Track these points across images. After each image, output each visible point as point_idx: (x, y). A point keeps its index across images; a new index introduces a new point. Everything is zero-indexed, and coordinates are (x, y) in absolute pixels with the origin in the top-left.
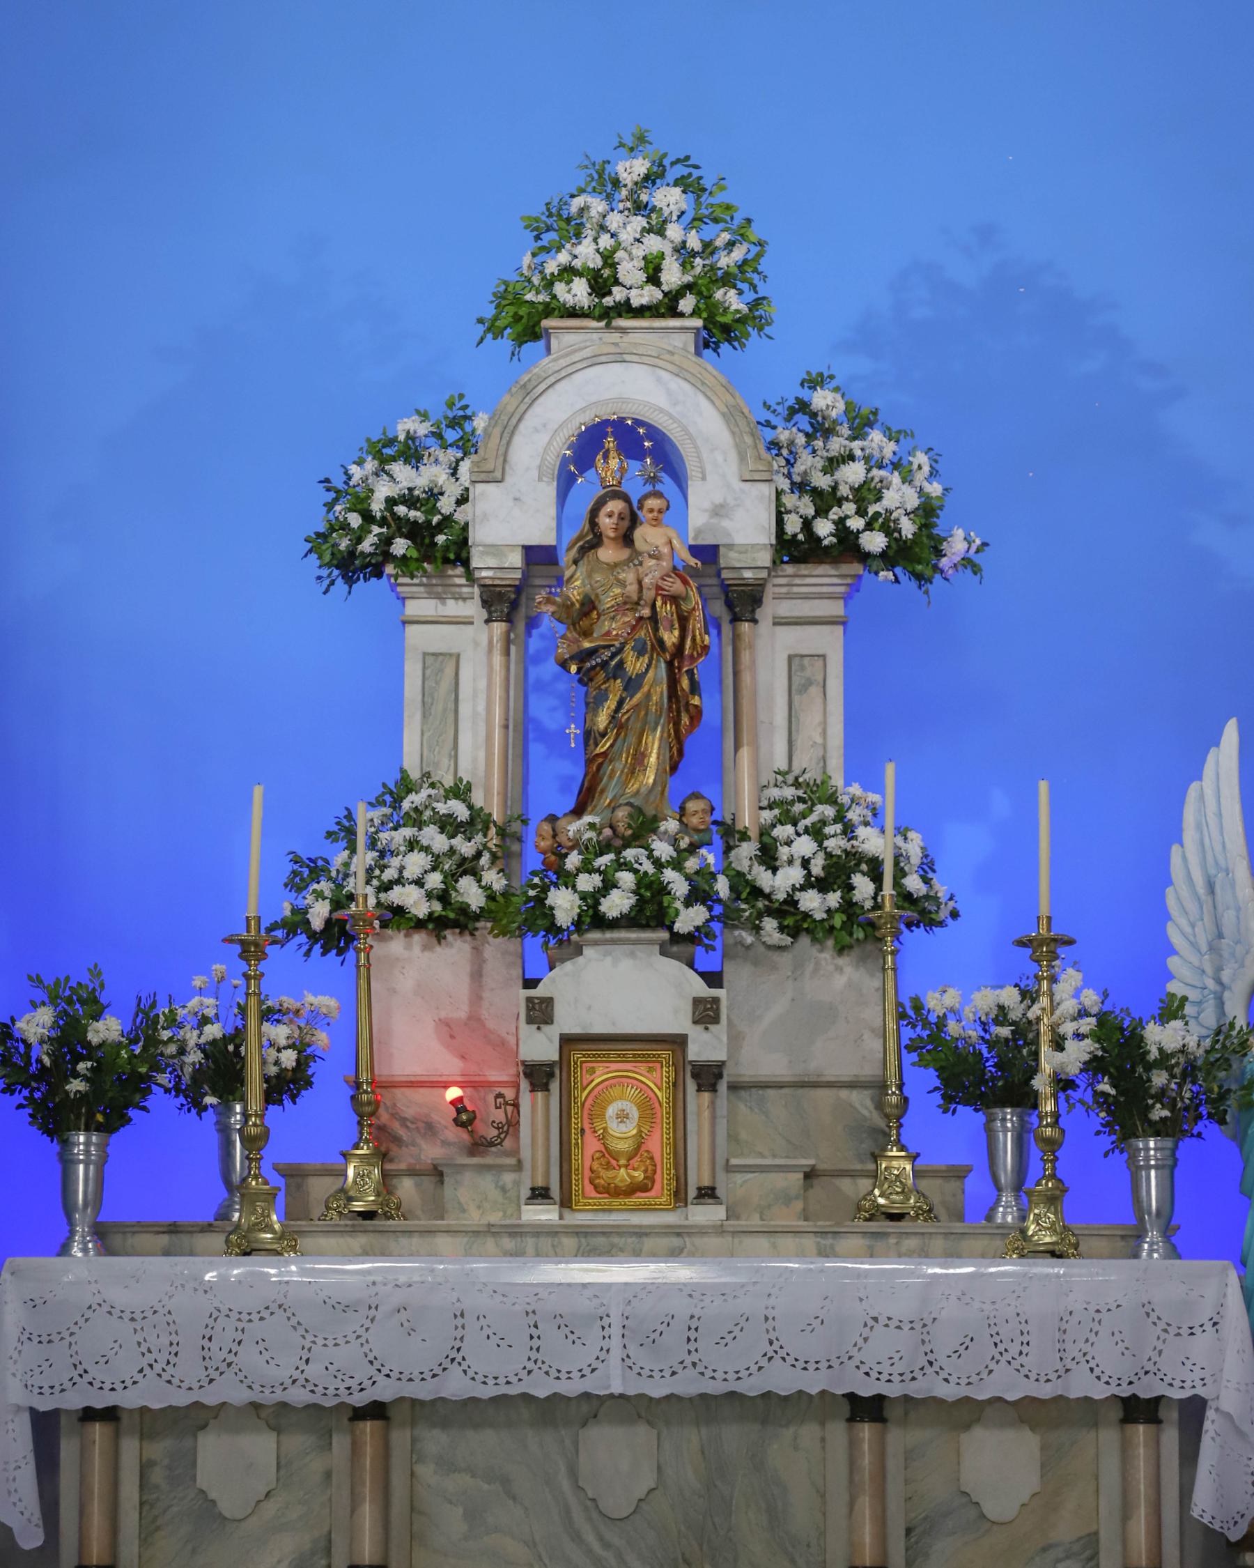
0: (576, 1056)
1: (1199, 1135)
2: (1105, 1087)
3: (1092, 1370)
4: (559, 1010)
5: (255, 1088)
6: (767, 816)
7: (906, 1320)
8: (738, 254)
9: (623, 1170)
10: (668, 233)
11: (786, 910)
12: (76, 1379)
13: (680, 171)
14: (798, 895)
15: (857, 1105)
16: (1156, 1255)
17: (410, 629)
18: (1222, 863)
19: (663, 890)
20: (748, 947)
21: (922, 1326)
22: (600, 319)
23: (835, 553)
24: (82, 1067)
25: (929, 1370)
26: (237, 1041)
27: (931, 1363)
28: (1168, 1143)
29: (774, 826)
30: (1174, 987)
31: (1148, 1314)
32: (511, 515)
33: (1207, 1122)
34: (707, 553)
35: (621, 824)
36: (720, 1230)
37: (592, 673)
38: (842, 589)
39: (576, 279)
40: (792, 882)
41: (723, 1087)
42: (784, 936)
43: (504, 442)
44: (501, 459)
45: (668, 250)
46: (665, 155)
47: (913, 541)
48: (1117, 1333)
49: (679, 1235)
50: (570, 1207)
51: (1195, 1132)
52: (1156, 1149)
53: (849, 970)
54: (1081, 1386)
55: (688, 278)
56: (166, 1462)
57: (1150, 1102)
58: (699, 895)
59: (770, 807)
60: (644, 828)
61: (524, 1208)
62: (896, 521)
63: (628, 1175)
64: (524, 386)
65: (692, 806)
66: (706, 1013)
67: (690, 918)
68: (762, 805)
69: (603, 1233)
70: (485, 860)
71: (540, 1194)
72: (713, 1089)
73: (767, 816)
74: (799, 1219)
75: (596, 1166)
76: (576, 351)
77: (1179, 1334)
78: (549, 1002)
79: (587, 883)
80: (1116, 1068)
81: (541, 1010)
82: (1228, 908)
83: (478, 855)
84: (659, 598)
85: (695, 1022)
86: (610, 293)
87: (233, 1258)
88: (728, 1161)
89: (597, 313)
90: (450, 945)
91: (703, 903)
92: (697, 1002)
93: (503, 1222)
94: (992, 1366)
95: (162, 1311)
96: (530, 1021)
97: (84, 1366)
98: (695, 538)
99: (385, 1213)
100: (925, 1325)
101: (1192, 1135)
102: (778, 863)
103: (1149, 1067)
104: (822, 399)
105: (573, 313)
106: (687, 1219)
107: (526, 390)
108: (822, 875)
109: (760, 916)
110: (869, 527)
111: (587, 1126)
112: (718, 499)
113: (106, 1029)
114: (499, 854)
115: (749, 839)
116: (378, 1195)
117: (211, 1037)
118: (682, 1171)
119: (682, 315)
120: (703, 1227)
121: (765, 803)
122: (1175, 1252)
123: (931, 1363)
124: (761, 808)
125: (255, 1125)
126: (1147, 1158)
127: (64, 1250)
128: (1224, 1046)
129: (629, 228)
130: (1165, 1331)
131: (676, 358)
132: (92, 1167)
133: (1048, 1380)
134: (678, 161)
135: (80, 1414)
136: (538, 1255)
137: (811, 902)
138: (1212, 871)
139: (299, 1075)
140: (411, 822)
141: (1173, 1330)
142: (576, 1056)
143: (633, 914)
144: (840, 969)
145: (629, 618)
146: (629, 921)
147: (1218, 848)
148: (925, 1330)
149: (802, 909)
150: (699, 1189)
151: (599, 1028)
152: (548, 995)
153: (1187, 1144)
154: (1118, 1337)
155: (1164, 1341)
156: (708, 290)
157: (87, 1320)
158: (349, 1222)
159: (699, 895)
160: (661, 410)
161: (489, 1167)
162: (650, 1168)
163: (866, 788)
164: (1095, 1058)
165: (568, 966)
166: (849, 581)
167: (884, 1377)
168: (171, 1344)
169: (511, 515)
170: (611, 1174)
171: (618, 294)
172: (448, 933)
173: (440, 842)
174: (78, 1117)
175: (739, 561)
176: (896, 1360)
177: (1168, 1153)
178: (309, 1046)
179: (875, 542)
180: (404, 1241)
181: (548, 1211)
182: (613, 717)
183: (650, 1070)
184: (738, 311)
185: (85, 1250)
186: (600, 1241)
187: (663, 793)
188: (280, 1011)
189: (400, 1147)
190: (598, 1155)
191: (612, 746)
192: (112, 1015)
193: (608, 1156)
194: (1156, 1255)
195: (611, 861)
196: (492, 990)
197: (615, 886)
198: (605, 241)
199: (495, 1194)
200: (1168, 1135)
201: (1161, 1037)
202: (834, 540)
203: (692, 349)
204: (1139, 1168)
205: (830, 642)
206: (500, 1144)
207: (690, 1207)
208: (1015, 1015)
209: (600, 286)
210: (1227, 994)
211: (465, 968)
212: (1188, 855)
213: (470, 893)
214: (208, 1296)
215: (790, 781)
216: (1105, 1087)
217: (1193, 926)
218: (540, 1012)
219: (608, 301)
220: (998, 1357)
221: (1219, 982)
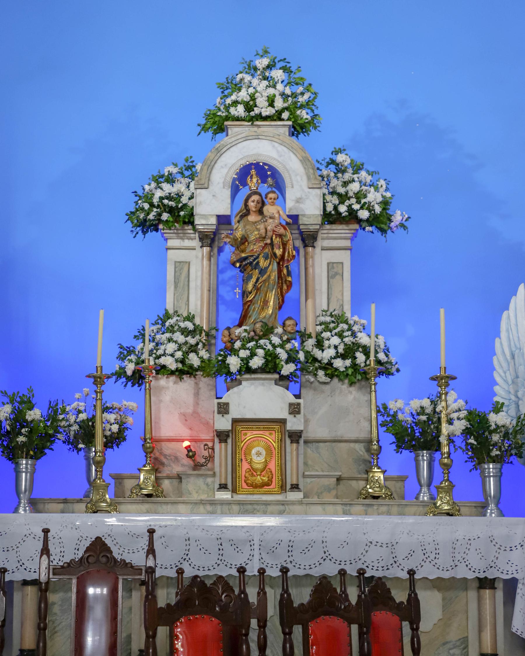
0: (239, 428)
1: (511, 463)
2: (472, 441)
3: (467, 566)
4: (232, 408)
5: (99, 440)
6: (319, 328)
7: (385, 543)
8: (306, 97)
9: (259, 477)
10: (277, 87)
12: (19, 567)
13: (282, 64)
14: (333, 361)
15: (358, 450)
16: (493, 515)
17: (169, 252)
18: (518, 346)
19: (276, 357)
20: (312, 383)
21: (392, 546)
22: (249, 121)
23: (347, 219)
24: (23, 430)
25: (395, 565)
26: (93, 421)
27: (395, 562)
28: (499, 466)
29: (322, 333)
30: (496, 399)
31: (492, 541)
32: (211, 203)
33: (515, 457)
34: (295, 218)
36: (300, 503)
37: (246, 267)
38: (350, 235)
39: (239, 105)
40: (330, 355)
41: (301, 441)
43: (209, 172)
44: (208, 179)
45: (277, 94)
46: (276, 58)
47: (380, 214)
48: (478, 549)
49: (283, 505)
50: (236, 493)
51: (510, 462)
52: (493, 468)
53: (354, 392)
54: (462, 573)
55: (286, 105)
56: (60, 603)
57: (491, 448)
58: (291, 359)
59: (321, 324)
60: (268, 332)
61: (216, 493)
62: (373, 206)
63: (261, 479)
64: (217, 149)
65: (288, 323)
66: (295, 409)
67: (288, 369)
69: (250, 504)
70: (200, 346)
71: (223, 487)
72: (298, 442)
73: (319, 328)
74: (334, 498)
75: (247, 475)
76: (239, 134)
77: (505, 550)
78: (227, 404)
79: (244, 354)
80: (476, 433)
81: (224, 408)
82: (521, 365)
83: (197, 344)
84: (274, 235)
85: (290, 414)
86: (253, 110)
87: (89, 514)
88: (304, 473)
89: (248, 119)
91: (293, 362)
92: (291, 405)
93: (207, 499)
94: (423, 563)
95: (57, 537)
96: (219, 413)
97: (23, 561)
98: (289, 212)
99: (157, 495)
100: (393, 545)
101: (508, 463)
102: (324, 348)
103: (491, 432)
104: (340, 158)
105: (238, 119)
106: (286, 498)
107: (218, 150)
108: (343, 352)
109: (316, 370)
110: (362, 208)
111: (243, 458)
112: (298, 195)
113: (34, 414)
114: (206, 344)
115: (312, 338)
116: (153, 487)
117: (82, 419)
118: (284, 477)
119: (283, 120)
120: (293, 501)
121: (318, 323)
122: (502, 513)
123: (395, 562)
124: (317, 325)
125: (99, 456)
126: (489, 473)
127: (16, 510)
128: (522, 423)
129: (261, 85)
130: (499, 548)
131: (281, 137)
132: (28, 474)
133: (448, 570)
134: (281, 60)
135: (22, 582)
136: (222, 513)
137: (339, 363)
138: (514, 349)
139: (120, 436)
140: (169, 331)
141: (503, 548)
142: (239, 428)
143: (263, 367)
144: (351, 393)
145: (262, 244)
146: (262, 370)
147: (516, 339)
148: (393, 547)
149: (335, 367)
150: (292, 485)
151: (249, 415)
152: (227, 402)
153: (506, 466)
154: (478, 551)
155: (499, 553)
156: (294, 110)
157: (24, 541)
158: (141, 499)
159: (291, 359)
160: (275, 159)
161: (201, 475)
163: (360, 318)
164: (467, 428)
165: (235, 389)
166: (353, 232)
167: (375, 568)
168: (61, 552)
169: (211, 203)
170: (254, 478)
171: (257, 111)
172: (184, 376)
174: (22, 452)
175: (308, 221)
176: (380, 561)
177: (498, 470)
178: (125, 423)
179: (364, 214)
180: (164, 507)
181: (227, 494)
182: (255, 285)
183: (270, 434)
184: (307, 119)
185: (25, 510)
186: (249, 507)
187: (275, 318)
188: (112, 408)
189: (164, 467)
190: (248, 470)
191: (254, 297)
192: (37, 408)
193: (252, 471)
194: (493, 515)
196: (203, 400)
197: (256, 355)
198: (251, 90)
199: (204, 487)
200: (499, 462)
201: (494, 419)
202: (347, 214)
203: (288, 134)
204: (486, 477)
205: (345, 257)
206: (206, 465)
207: (288, 493)
208: (429, 410)
209: (249, 108)
210: (520, 402)
211: (192, 391)
212: (503, 342)
213: (194, 360)
214: (77, 531)
215: (328, 313)
216: (472, 441)
217: (505, 373)
218: (223, 409)
219: (252, 114)
220: (425, 559)
221: (517, 397)
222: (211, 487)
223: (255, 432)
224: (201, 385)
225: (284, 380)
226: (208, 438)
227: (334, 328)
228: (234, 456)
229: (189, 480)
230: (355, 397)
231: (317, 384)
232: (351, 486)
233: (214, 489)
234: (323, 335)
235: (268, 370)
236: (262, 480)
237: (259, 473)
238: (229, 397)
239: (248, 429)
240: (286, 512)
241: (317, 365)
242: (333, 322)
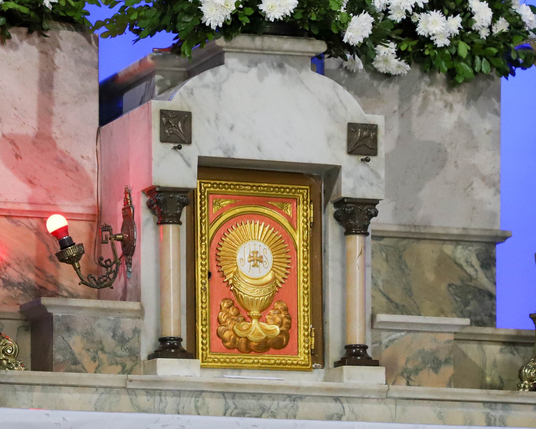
4: (198, 128)
15: (462, 262)
49: (337, 399)
53: (459, 108)
66: (362, 141)
69: (254, 395)
74: (449, 385)
90: (15, 47)
96: (164, 139)
111: (215, 270)
144: (449, 106)
146: (287, 27)
162: (286, 320)
165: (208, 76)
170: (245, 326)
186: (251, 403)
196: (64, 103)
211: (33, 76)
224: (60, 58)
226: (80, 210)
230: (460, 118)
232: (465, 356)
236: (266, 331)
237: (255, 312)
238: (195, 94)
240: (344, 418)
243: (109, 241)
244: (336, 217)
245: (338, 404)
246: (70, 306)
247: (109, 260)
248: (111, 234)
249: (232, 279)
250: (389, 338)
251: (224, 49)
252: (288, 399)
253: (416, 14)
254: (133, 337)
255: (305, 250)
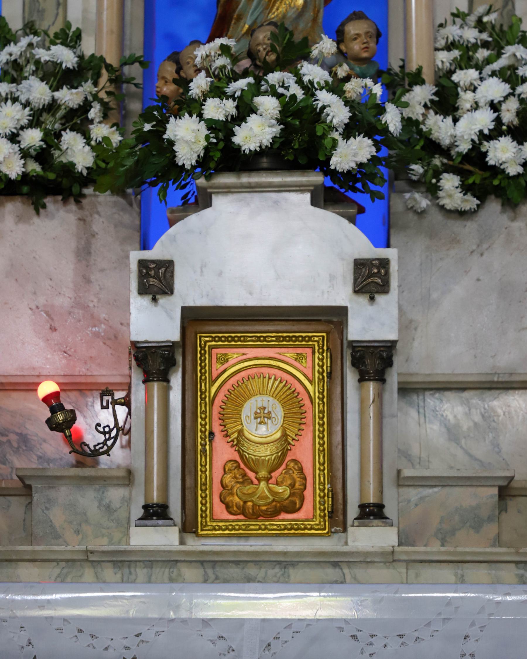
6: (445, 58)
9: (263, 484)
11: (473, 166)
14: (486, 146)
19: (317, 115)
20: (421, 214)
29: (451, 72)
35: (261, 48)
40: (477, 128)
41: (393, 378)
42: (469, 197)
50: (196, 533)
58: (363, 121)
59: (450, 46)
60: (292, 52)
61: (133, 530)
63: (270, 490)
65: (353, 29)
66: (370, 279)
67: (351, 153)
68: (438, 45)
71: (156, 513)
72: (380, 378)
74: (493, 546)
75: (228, 479)
78: (168, 265)
81: (157, 277)
83: (86, 107)
85: (357, 292)
88: (399, 472)
90: (52, 217)
91: (369, 135)
96: (143, 291)
102: (458, 114)
106: (346, 543)
109: (437, 174)
111: (217, 429)
114: (112, 105)
115: (422, 82)
118: (339, 486)
121: (442, 43)
140: (8, 78)
143: (276, 146)
149: (491, 162)
150: (362, 507)
151: (234, 298)
152: (167, 257)
159: (363, 121)
170: (248, 489)
172: (48, 201)
173: (37, 91)
183: (299, 357)
190: (229, 465)
193: (244, 465)
195: (249, 84)
197: (253, 110)
206: (107, 453)
207: (350, 529)
213: (77, 152)
215: (472, 19)
222: (122, 514)
223: (252, 353)
225: (337, 193)
227: (488, 61)
228: (188, 424)
229: (52, 494)
231: (436, 217)
233: (129, 522)
234: (455, 78)
235: (291, 158)
237: (263, 473)
239: (233, 342)
241: (437, 161)
242: (485, 45)
243: (110, 406)
244: (353, 364)
245: (338, 570)
246: (47, 476)
247: (108, 426)
248: (113, 398)
249: (237, 438)
250: (419, 496)
251: (209, 190)
252: (278, 566)
253: (485, 143)
254: (120, 507)
255: (320, 402)
